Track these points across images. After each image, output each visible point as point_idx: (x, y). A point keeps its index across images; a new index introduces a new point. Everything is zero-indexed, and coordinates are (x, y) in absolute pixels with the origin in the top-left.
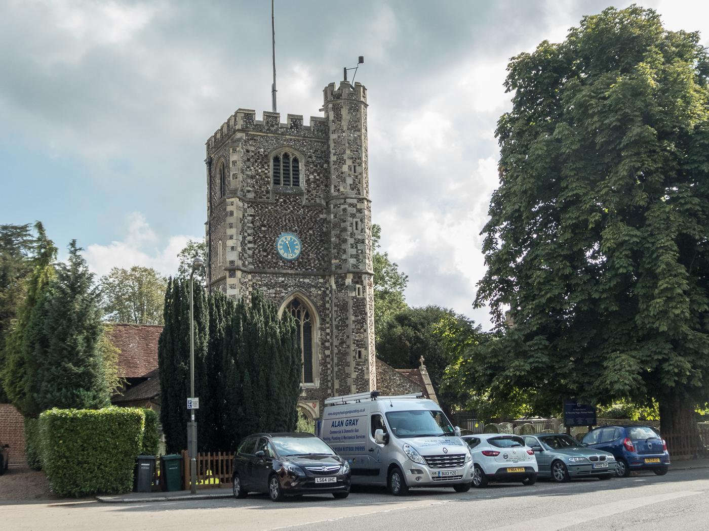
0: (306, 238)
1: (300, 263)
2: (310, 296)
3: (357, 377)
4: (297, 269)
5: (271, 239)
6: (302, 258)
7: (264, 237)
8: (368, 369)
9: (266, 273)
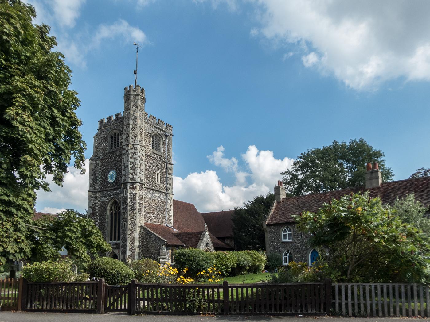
1: (116, 183)
2: (119, 198)
6: (117, 181)
7: (104, 174)
8: (127, 233)
9: (104, 191)
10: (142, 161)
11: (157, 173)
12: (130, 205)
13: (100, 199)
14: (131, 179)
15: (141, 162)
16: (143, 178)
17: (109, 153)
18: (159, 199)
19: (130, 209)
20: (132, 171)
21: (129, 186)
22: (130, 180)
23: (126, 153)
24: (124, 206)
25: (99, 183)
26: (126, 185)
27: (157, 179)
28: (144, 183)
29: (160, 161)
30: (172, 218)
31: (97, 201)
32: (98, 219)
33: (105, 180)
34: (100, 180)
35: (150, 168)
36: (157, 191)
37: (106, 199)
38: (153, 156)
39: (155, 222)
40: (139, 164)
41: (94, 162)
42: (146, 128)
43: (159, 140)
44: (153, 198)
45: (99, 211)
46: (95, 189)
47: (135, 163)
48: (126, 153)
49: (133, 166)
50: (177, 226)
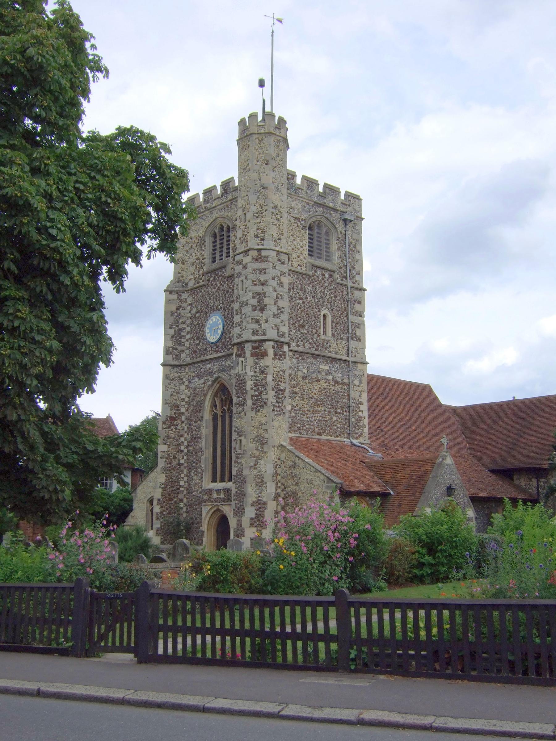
0: (228, 314)
1: (223, 344)
3: (237, 474)
4: (220, 352)
5: (202, 324)
7: (198, 324)
10: (281, 289)
11: (322, 313)
12: (253, 396)
13: (189, 382)
14: (255, 333)
15: (279, 289)
16: (284, 329)
17: (207, 273)
18: (330, 378)
19: (254, 404)
20: (257, 314)
21: (248, 348)
22: (253, 334)
23: (244, 272)
24: (238, 397)
25: (187, 344)
26: (243, 348)
27: (324, 328)
28: (287, 340)
29: (330, 284)
30: (366, 422)
31: (183, 387)
32: (186, 429)
33: (200, 336)
34: (188, 336)
35: (303, 302)
36: (324, 356)
37: (202, 381)
38: (311, 273)
39: (319, 434)
40: (274, 295)
41: (175, 296)
42: (293, 208)
43: (327, 233)
44: (314, 376)
45: (187, 410)
46: (177, 358)
47: (265, 293)
48: (244, 272)
49: (260, 300)
50: (380, 442)
